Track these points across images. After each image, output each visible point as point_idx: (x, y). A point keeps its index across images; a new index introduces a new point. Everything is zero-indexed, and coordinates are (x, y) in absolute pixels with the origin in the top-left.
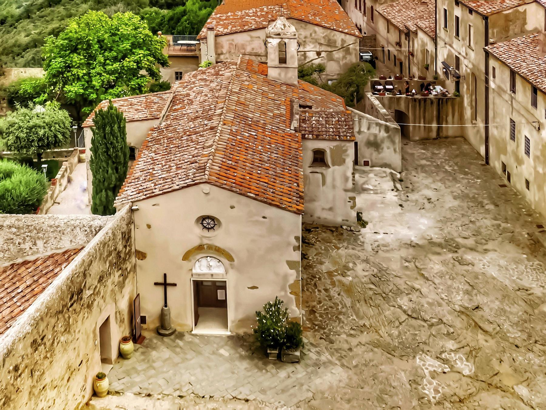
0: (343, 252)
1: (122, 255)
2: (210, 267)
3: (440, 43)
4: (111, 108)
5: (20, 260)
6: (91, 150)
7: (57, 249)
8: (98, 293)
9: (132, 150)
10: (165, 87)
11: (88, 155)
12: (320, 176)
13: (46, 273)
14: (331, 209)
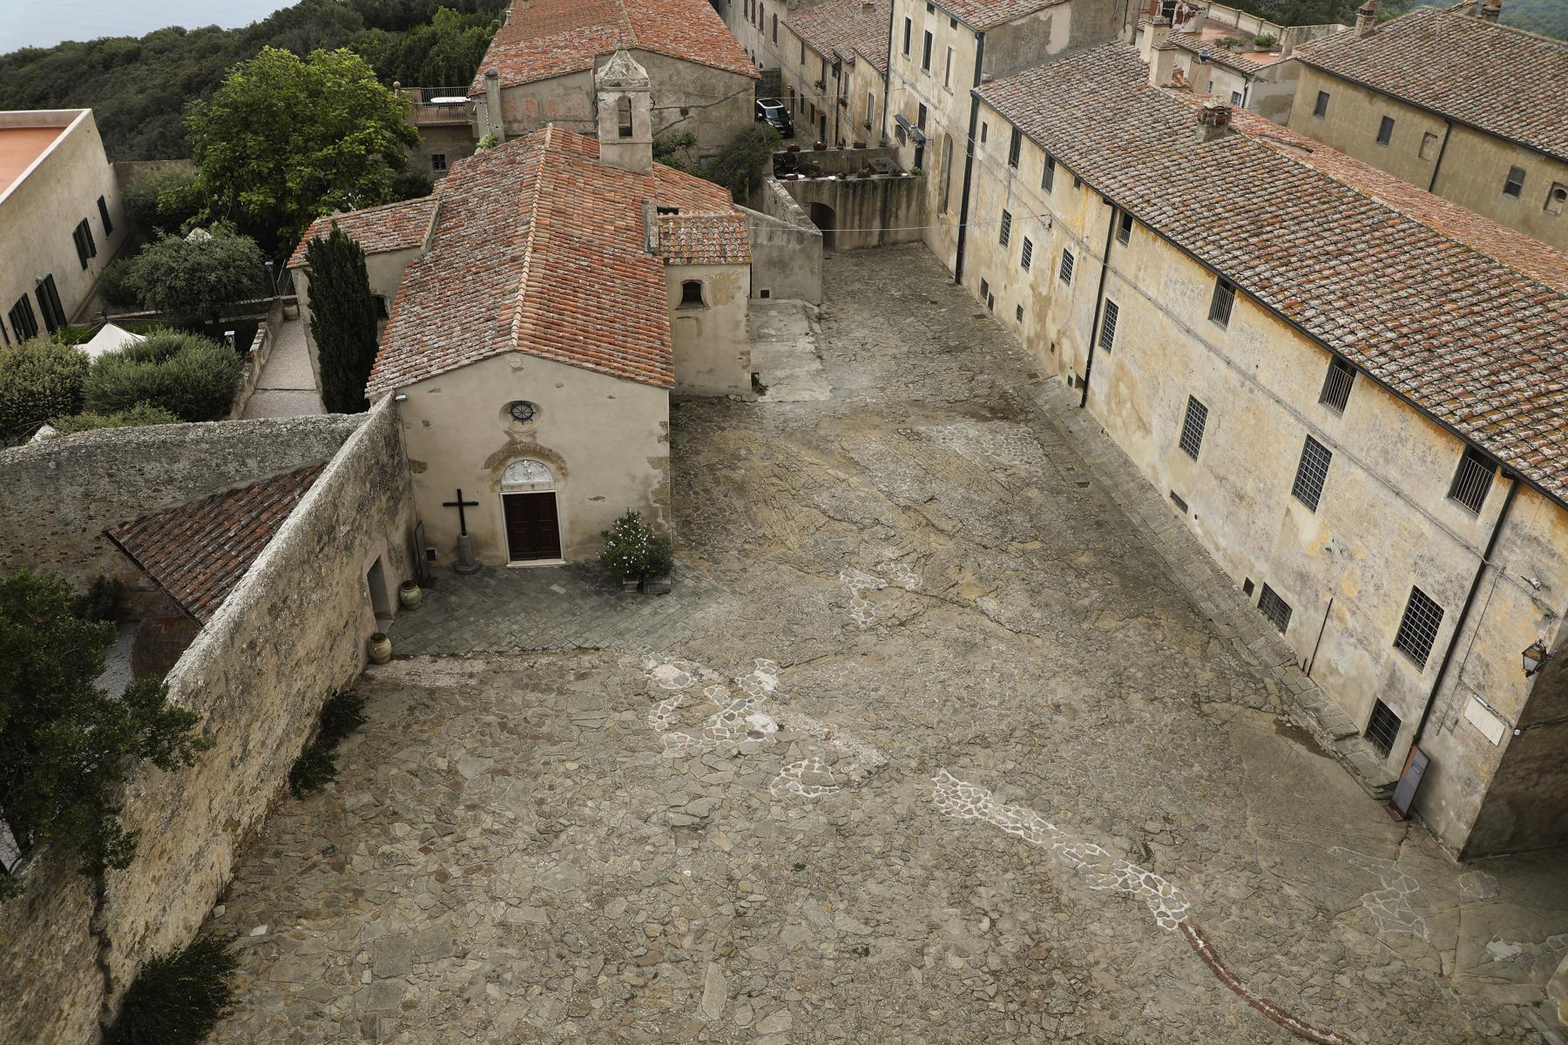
0: (732, 436)
1: (389, 470)
2: (528, 475)
3: (896, 82)
4: (335, 234)
5: (224, 490)
6: (309, 306)
7: (280, 468)
8: (360, 527)
9: (380, 300)
10: (419, 188)
11: (306, 312)
12: (693, 322)
13: (270, 506)
14: (711, 371)
